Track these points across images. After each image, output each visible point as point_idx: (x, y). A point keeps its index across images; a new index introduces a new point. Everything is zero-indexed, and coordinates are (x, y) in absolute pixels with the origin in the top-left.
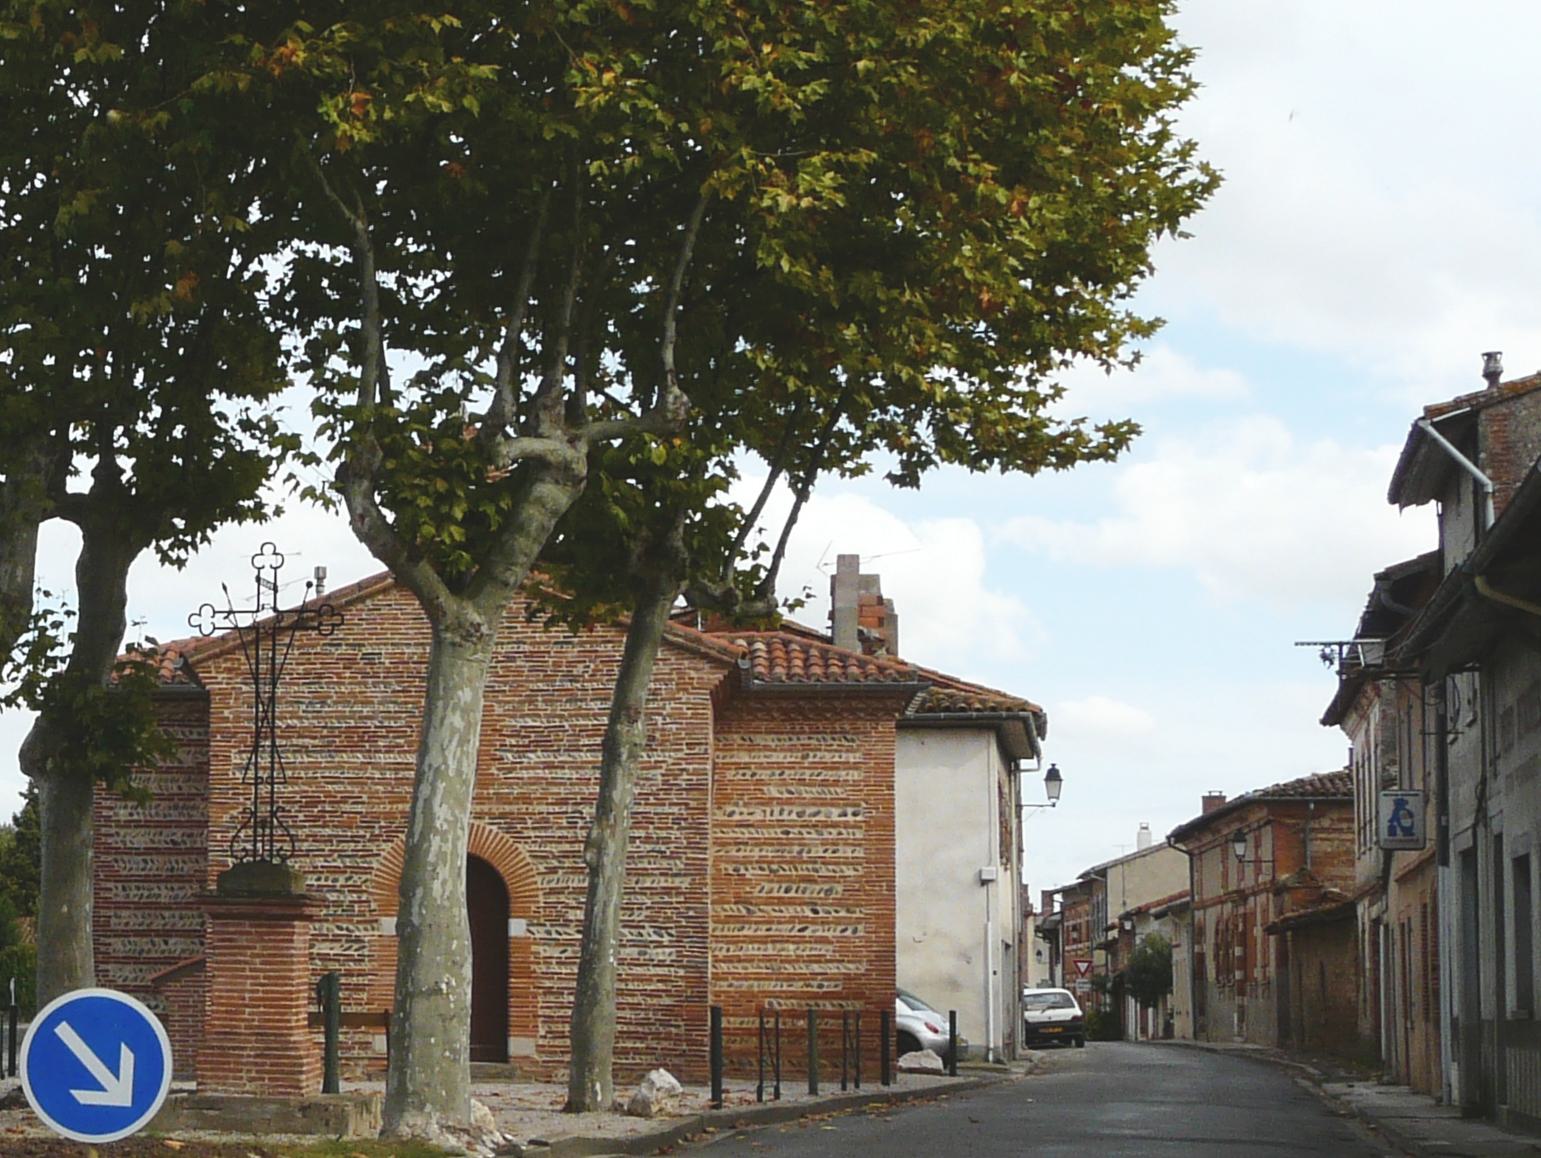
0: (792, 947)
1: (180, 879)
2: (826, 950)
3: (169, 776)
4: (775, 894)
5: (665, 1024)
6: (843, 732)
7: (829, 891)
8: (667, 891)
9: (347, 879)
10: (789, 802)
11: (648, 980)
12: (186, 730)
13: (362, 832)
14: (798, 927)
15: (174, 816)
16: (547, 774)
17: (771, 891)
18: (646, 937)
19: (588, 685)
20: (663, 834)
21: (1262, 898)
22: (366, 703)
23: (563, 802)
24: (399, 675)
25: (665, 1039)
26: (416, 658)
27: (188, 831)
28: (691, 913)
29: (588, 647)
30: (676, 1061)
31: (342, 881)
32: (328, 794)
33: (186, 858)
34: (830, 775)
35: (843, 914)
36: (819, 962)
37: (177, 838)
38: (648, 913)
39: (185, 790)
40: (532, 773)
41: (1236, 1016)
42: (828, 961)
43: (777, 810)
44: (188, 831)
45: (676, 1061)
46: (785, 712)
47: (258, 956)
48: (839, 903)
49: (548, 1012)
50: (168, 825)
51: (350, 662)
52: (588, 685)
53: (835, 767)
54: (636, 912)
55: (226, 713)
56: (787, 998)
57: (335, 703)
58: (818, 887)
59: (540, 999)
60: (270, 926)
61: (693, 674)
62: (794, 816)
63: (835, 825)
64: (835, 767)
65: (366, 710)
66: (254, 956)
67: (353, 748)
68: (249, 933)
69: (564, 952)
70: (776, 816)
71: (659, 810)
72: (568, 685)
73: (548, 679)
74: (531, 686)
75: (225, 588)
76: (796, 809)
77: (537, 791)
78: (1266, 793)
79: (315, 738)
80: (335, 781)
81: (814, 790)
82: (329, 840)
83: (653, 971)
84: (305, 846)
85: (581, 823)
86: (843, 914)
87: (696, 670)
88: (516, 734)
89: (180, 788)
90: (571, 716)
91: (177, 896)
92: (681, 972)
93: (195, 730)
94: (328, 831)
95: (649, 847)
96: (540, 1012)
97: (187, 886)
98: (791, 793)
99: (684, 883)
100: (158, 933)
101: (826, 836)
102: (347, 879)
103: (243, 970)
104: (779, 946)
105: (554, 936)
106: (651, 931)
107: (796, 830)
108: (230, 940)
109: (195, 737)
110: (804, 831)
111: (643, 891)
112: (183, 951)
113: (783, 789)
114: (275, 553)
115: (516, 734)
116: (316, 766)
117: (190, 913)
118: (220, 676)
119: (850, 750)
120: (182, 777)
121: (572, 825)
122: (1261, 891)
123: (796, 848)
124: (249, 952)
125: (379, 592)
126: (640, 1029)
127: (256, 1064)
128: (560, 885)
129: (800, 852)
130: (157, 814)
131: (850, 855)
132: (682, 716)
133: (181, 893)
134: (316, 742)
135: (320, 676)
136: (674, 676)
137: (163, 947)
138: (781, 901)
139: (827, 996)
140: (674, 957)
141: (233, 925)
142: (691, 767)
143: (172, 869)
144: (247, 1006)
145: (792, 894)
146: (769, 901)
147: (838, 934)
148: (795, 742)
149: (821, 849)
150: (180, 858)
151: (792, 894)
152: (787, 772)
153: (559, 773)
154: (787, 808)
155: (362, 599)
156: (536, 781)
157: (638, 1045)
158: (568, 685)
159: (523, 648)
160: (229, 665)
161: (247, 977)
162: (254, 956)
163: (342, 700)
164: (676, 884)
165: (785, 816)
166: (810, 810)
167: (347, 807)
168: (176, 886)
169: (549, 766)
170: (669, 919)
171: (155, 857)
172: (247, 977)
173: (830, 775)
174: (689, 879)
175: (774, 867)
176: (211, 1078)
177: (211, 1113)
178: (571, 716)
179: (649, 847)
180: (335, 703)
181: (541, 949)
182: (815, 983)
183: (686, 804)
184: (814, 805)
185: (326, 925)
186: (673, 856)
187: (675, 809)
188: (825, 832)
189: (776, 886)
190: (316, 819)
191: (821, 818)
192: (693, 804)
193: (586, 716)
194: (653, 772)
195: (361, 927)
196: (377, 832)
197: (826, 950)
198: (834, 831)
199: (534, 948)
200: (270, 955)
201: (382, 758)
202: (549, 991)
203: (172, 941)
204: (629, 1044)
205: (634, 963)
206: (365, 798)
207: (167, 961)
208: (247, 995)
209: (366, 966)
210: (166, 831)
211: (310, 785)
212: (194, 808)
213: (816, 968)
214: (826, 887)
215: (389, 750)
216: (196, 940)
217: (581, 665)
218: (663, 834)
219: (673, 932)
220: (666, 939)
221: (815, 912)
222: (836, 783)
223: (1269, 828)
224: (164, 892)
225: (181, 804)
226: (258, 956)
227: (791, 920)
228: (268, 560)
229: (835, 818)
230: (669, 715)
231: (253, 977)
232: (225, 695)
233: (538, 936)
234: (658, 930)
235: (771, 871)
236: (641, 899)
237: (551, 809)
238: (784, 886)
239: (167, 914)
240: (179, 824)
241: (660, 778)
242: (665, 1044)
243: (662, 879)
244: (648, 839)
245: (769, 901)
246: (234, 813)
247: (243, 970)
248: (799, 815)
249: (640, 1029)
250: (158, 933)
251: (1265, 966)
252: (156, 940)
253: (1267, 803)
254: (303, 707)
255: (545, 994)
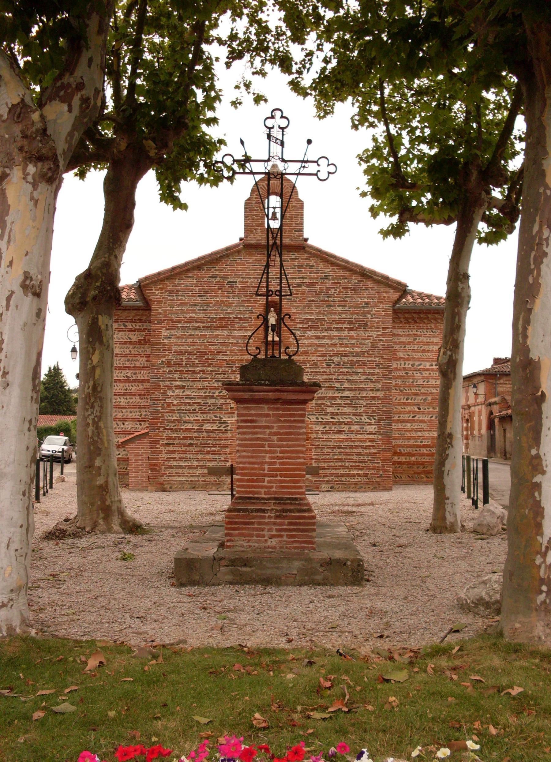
0: (409, 425)
1: (130, 394)
2: (424, 426)
3: (125, 346)
4: (402, 401)
5: (372, 462)
6: (431, 328)
7: (425, 400)
8: (373, 398)
9: (220, 393)
10: (408, 359)
11: (364, 441)
12: (134, 324)
13: (227, 370)
14: (412, 415)
15: (128, 364)
16: (316, 341)
17: (400, 399)
18: (363, 420)
19: (337, 299)
20: (372, 371)
21: (477, 408)
22: (229, 306)
23: (324, 355)
24: (245, 293)
25: (373, 469)
26: (253, 285)
27: (134, 372)
28: (384, 409)
29: (336, 281)
30: (378, 480)
31: (217, 393)
32: (210, 351)
33: (133, 384)
34: (426, 348)
35: (431, 409)
36: (420, 431)
37: (129, 375)
38: (364, 408)
39: (132, 353)
40: (310, 341)
41: (464, 447)
42: (425, 431)
43: (403, 363)
44: (134, 372)
45: (378, 480)
46: (406, 319)
47: (275, 434)
48: (429, 404)
49: (317, 457)
50: (124, 368)
51: (221, 286)
52: (337, 299)
53: (428, 344)
54: (359, 408)
55: (160, 310)
56: (407, 447)
57: (214, 305)
58: (420, 398)
59: (313, 451)
60: (284, 410)
61: (385, 295)
62: (410, 366)
63: (427, 370)
64: (428, 344)
65: (229, 310)
66: (271, 434)
67: (222, 328)
68: (268, 415)
69: (325, 427)
70: (402, 366)
71: (370, 359)
72: (326, 299)
73: (317, 295)
74: (309, 299)
75: (242, 142)
76: (411, 363)
77: (311, 350)
78: (484, 371)
79: (204, 323)
80: (213, 344)
81: (419, 354)
82: (211, 373)
83: (367, 436)
84: (199, 376)
85: (333, 365)
86: (431, 409)
87: (386, 292)
88: (302, 322)
89: (130, 351)
90: (328, 313)
91: (129, 402)
92: (380, 437)
93: (137, 324)
94: (209, 369)
95: (365, 377)
96: (314, 457)
97: (134, 397)
98: (408, 355)
99: (381, 394)
100: (120, 420)
101: (424, 375)
102: (220, 393)
103: (263, 446)
104: (404, 424)
105: (320, 420)
106: (366, 417)
107: (411, 372)
108: (252, 421)
109: (138, 327)
110: (414, 372)
111: (362, 398)
112: (132, 428)
113: (405, 354)
114: (282, 117)
115: (302, 322)
116: (205, 336)
117: (135, 410)
118: (157, 292)
119: (434, 336)
120: (131, 346)
121: (329, 366)
122: (478, 405)
123: (411, 380)
124: (268, 431)
125: (235, 252)
126: (361, 465)
127: (275, 524)
128: (323, 395)
129: (413, 382)
130: (120, 364)
131: (434, 383)
132: (380, 314)
133: (131, 401)
134: (204, 325)
135: (206, 293)
136: (377, 296)
137: (122, 426)
138: (404, 404)
139: (425, 446)
140: (376, 430)
141: (255, 409)
142: (384, 339)
143: (126, 390)
144: (265, 475)
145: (409, 401)
146: (400, 404)
147: (429, 418)
148: (410, 333)
149: (422, 381)
150: (130, 384)
151: (409, 401)
152: (407, 346)
153: (323, 341)
154: (407, 362)
155: (227, 256)
156: (311, 345)
157: (360, 472)
158: (326, 299)
159: (305, 280)
160: (161, 286)
161: (266, 452)
162: (271, 434)
163: (218, 304)
164: (378, 395)
165: (406, 366)
166: (417, 363)
167: (219, 357)
168: (128, 397)
169: (317, 338)
170: (374, 412)
171: (118, 384)
172: (266, 452)
173: (426, 348)
174: (383, 393)
175: (402, 389)
176: (239, 535)
177: (244, 569)
178: (328, 313)
179: (365, 377)
180: (214, 305)
181: (313, 426)
182: (419, 441)
183: (382, 357)
184: (419, 361)
185: (209, 415)
186: (377, 381)
187: (377, 359)
188: (424, 373)
189: (402, 397)
190: (204, 363)
191: (422, 367)
192: (385, 357)
193: (335, 314)
194: (367, 341)
195: (226, 416)
196: (234, 369)
197: (424, 426)
198: (428, 373)
199: (310, 426)
200: (286, 434)
201: (236, 333)
202: (317, 447)
203: (126, 423)
204: (355, 472)
205: (358, 433)
206: (228, 353)
207: (125, 433)
208: (266, 467)
209: (229, 435)
210: (124, 372)
211: (201, 346)
212: (137, 360)
213: (419, 434)
214: (424, 397)
215: (240, 329)
216: (138, 423)
217: (333, 290)
218: (372, 371)
219: (376, 418)
220: (373, 421)
221: (419, 409)
222: (428, 351)
223: (483, 383)
224: (123, 400)
225: (131, 359)
226: (275, 434)
227: (409, 412)
228: (279, 121)
229: (428, 367)
230: (374, 314)
231: (270, 452)
232: (159, 301)
233: (312, 420)
234: (369, 417)
235: (401, 391)
236: (361, 402)
237: (319, 358)
238: (406, 397)
239: (124, 410)
240: (129, 368)
241: (370, 344)
242: (372, 472)
243: (371, 392)
244: (364, 373)
245: (400, 404)
246: (164, 359)
247: (263, 446)
248: (413, 365)
249: (361, 465)
250: (120, 420)
251: (480, 430)
252: (119, 423)
253: (484, 374)
254: (198, 308)
255: (316, 448)
